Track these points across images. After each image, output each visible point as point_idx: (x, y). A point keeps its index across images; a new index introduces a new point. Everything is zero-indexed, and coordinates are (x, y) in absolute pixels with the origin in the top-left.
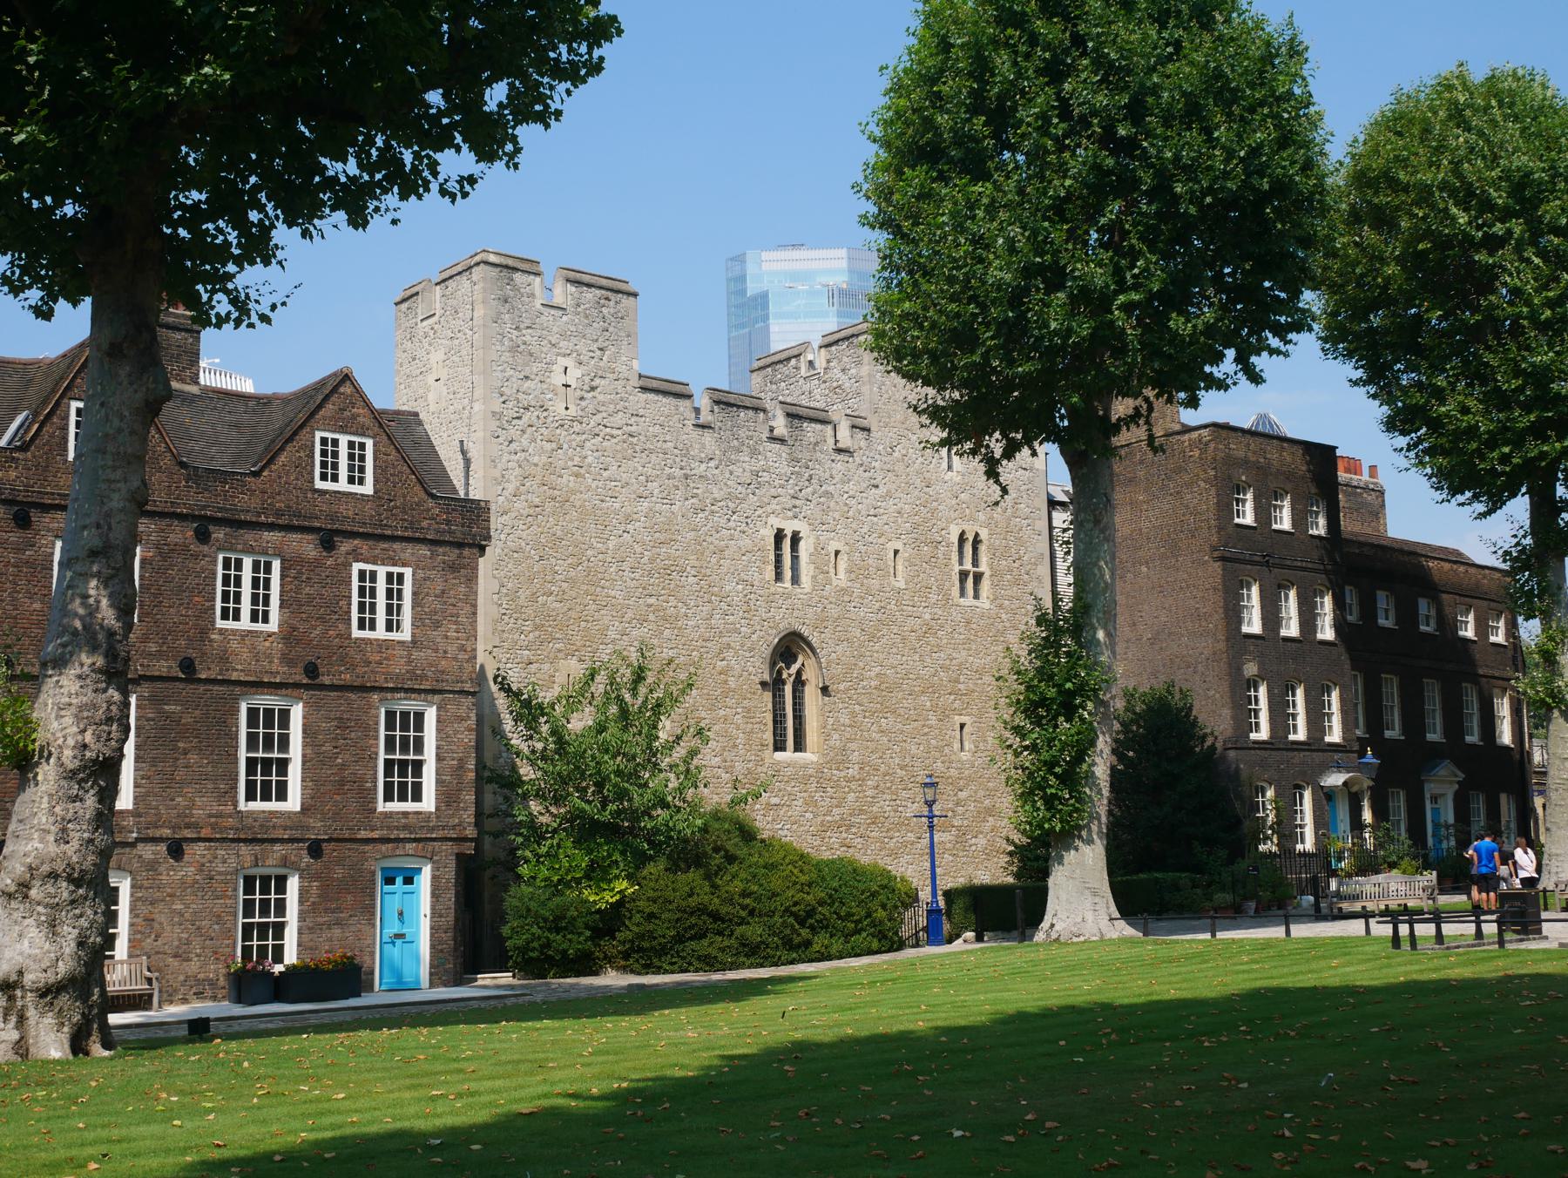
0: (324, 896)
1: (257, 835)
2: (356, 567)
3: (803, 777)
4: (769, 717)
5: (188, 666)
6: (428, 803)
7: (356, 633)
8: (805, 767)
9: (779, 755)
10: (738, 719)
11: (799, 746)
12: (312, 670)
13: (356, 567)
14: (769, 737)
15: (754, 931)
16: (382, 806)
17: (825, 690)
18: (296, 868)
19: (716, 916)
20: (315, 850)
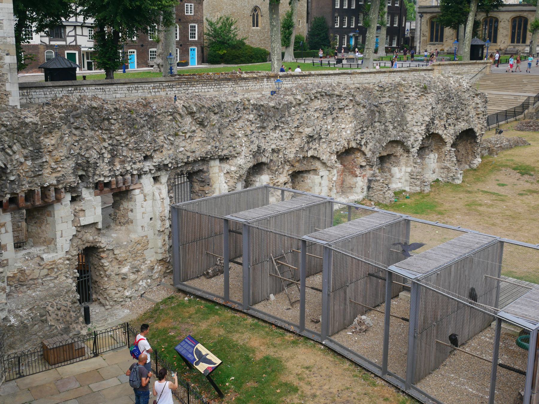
0: (183, 52)
2: (186, 4)
3: (257, 31)
4: (252, 21)
6: (196, 39)
7: (186, 14)
8: (258, 30)
9: (253, 28)
10: (246, 22)
11: (257, 26)
12: (180, 20)
13: (186, 4)
14: (252, 24)
15: (243, 59)
16: (190, 39)
17: (262, 16)
18: (178, 48)
19: (238, 57)
20: (181, 45)
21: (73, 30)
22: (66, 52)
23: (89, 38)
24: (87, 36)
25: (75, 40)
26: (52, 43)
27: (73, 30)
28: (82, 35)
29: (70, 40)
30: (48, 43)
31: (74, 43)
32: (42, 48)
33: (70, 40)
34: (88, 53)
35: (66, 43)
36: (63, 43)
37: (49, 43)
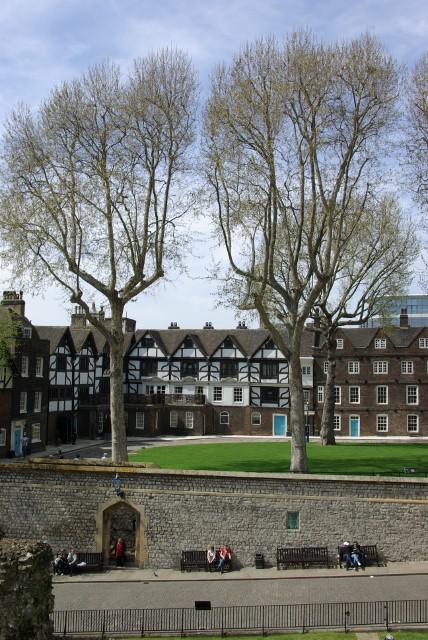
1: (411, 409)
5: (397, 381)
22: (274, 415)
31: (287, 406)
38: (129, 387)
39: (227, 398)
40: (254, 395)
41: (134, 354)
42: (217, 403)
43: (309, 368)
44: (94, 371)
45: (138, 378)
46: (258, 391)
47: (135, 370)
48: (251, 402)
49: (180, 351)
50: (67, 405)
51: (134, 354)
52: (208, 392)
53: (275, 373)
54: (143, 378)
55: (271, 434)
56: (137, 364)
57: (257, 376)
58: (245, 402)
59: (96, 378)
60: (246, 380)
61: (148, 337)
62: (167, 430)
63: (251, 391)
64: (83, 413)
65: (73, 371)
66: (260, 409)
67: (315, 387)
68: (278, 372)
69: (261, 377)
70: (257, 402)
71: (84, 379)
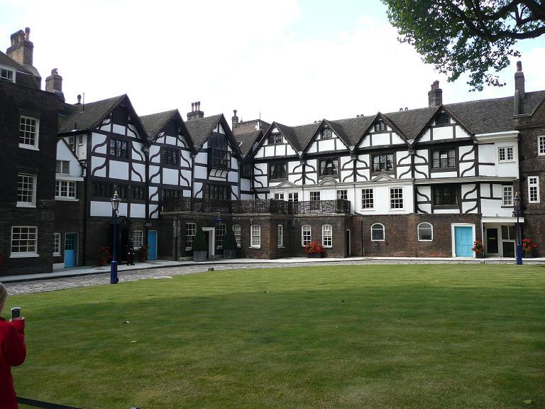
21: (474, 190)
22: (453, 225)
23: (505, 203)
24: (501, 199)
25: (478, 206)
26: (437, 212)
27: (474, 190)
28: (492, 198)
29: (466, 207)
30: (430, 212)
31: (476, 211)
32: (413, 218)
33: (466, 207)
34: (506, 227)
35: (461, 211)
36: (457, 211)
37: (432, 212)
38: (257, 197)
39: (382, 204)
40: (421, 199)
41: (260, 155)
42: (367, 212)
43: (510, 150)
44: (192, 170)
45: (265, 185)
46: (427, 192)
47: (262, 175)
48: (416, 208)
49: (315, 144)
50: (138, 211)
51: (260, 155)
52: (355, 198)
53: (452, 163)
54: (272, 184)
55: (451, 256)
56: (264, 167)
57: (425, 169)
58: (408, 208)
59: (194, 180)
60: (409, 176)
61: (275, 131)
62: (292, 249)
63: (416, 192)
64: (159, 225)
65: (147, 163)
66: (432, 218)
67: (522, 179)
68: (458, 162)
69: (431, 170)
70: (427, 208)
71: (170, 177)
